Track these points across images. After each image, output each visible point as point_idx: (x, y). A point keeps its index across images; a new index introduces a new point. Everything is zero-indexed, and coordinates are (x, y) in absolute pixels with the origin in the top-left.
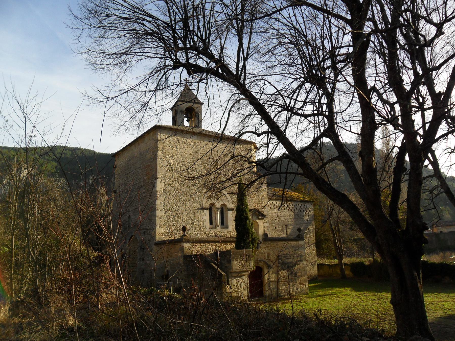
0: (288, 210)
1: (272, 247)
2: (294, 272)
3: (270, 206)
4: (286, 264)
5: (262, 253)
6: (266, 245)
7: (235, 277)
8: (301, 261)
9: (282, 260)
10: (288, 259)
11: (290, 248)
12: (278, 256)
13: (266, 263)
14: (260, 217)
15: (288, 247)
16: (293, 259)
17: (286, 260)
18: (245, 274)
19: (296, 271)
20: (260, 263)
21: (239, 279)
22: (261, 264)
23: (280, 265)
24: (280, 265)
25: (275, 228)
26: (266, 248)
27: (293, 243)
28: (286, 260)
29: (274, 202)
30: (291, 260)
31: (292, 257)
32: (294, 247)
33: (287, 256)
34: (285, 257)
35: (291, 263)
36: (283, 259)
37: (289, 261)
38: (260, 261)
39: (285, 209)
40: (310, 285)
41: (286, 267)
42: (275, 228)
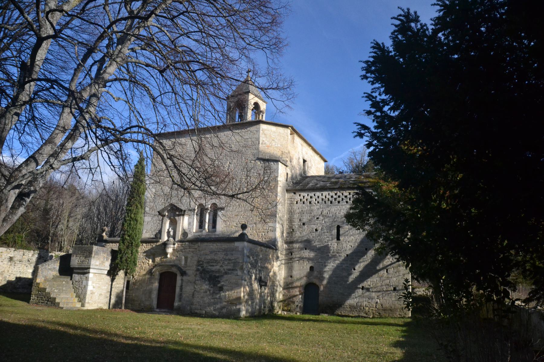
0: (347, 202)
1: (191, 250)
2: (219, 285)
3: (309, 199)
4: (208, 272)
7: (78, 273)
8: (233, 270)
9: (202, 267)
10: (213, 266)
11: (219, 251)
12: (199, 261)
13: (179, 269)
14: (177, 213)
15: (216, 250)
16: (221, 266)
17: (209, 267)
18: (85, 271)
19: (223, 283)
20: (173, 269)
21: (82, 276)
22: (174, 270)
23: (198, 273)
24: (198, 273)
25: (316, 230)
26: (184, 251)
27: (225, 245)
28: (209, 267)
29: (318, 194)
30: (218, 267)
31: (220, 265)
32: (225, 250)
33: (212, 263)
34: (208, 263)
35: (216, 272)
36: (205, 265)
37: (214, 268)
38: (172, 266)
39: (339, 202)
40: (238, 307)
41: (208, 276)
42: (316, 230)
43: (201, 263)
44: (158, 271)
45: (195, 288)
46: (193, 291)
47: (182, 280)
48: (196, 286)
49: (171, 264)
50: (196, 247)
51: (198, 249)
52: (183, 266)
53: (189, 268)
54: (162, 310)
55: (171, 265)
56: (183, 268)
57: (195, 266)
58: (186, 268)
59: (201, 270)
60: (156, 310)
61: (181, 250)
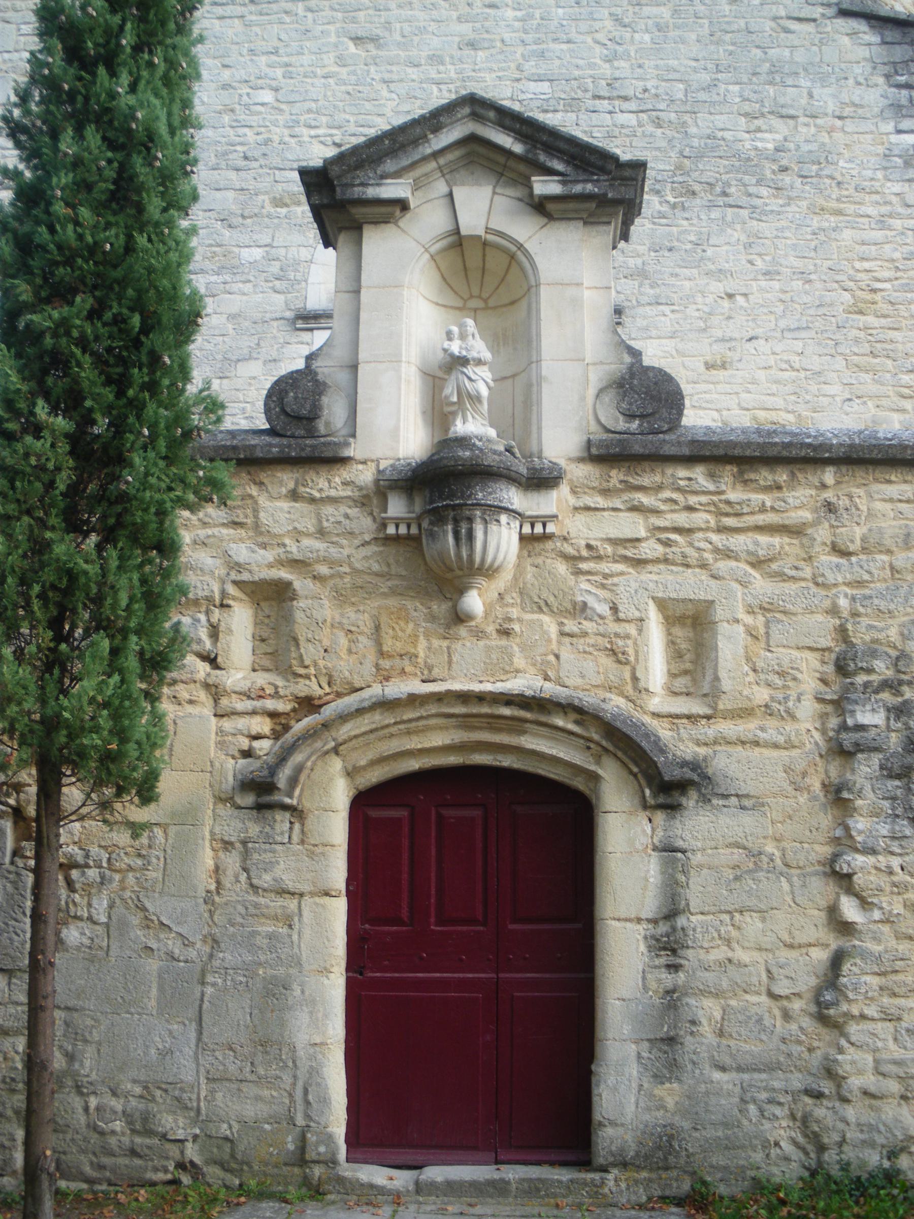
1: (739, 542)
5: (581, 610)
6: (635, 508)
43: (883, 669)
44: (350, 774)
45: (845, 928)
46: (820, 956)
47: (668, 849)
48: (850, 910)
49: (515, 685)
50: (806, 515)
51: (822, 534)
52: (656, 703)
53: (747, 728)
54: (436, 1173)
55: (508, 700)
56: (664, 732)
57: (807, 709)
58: (710, 731)
59: (894, 741)
60: (348, 1170)
61: (615, 542)
